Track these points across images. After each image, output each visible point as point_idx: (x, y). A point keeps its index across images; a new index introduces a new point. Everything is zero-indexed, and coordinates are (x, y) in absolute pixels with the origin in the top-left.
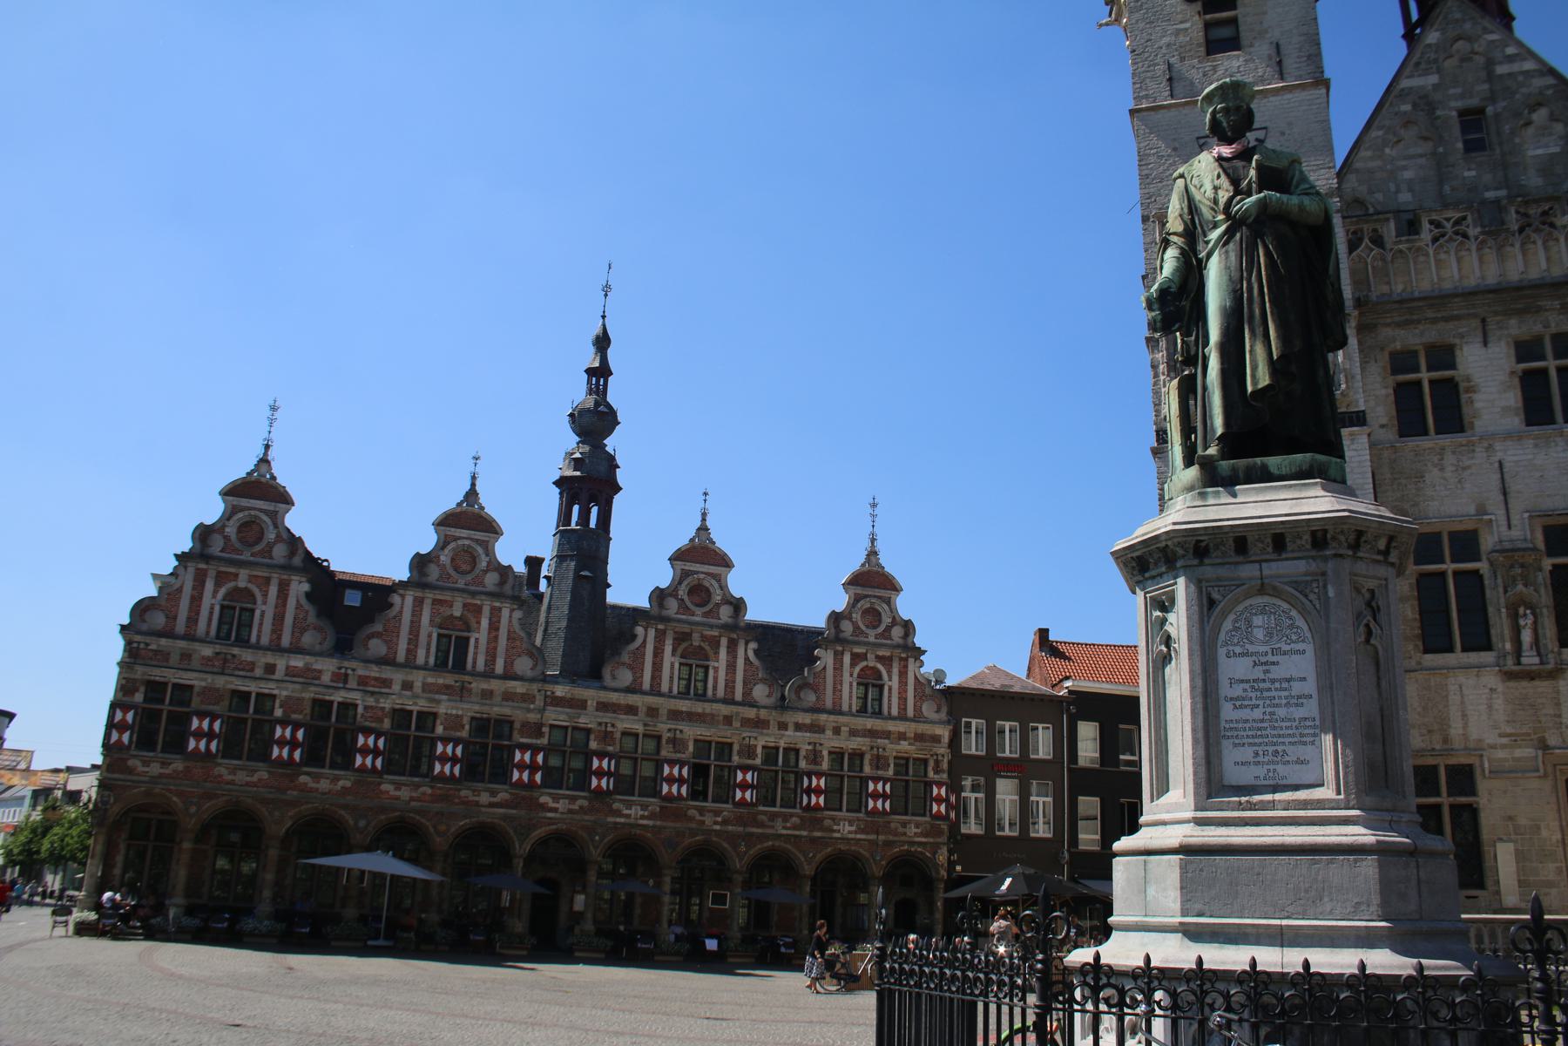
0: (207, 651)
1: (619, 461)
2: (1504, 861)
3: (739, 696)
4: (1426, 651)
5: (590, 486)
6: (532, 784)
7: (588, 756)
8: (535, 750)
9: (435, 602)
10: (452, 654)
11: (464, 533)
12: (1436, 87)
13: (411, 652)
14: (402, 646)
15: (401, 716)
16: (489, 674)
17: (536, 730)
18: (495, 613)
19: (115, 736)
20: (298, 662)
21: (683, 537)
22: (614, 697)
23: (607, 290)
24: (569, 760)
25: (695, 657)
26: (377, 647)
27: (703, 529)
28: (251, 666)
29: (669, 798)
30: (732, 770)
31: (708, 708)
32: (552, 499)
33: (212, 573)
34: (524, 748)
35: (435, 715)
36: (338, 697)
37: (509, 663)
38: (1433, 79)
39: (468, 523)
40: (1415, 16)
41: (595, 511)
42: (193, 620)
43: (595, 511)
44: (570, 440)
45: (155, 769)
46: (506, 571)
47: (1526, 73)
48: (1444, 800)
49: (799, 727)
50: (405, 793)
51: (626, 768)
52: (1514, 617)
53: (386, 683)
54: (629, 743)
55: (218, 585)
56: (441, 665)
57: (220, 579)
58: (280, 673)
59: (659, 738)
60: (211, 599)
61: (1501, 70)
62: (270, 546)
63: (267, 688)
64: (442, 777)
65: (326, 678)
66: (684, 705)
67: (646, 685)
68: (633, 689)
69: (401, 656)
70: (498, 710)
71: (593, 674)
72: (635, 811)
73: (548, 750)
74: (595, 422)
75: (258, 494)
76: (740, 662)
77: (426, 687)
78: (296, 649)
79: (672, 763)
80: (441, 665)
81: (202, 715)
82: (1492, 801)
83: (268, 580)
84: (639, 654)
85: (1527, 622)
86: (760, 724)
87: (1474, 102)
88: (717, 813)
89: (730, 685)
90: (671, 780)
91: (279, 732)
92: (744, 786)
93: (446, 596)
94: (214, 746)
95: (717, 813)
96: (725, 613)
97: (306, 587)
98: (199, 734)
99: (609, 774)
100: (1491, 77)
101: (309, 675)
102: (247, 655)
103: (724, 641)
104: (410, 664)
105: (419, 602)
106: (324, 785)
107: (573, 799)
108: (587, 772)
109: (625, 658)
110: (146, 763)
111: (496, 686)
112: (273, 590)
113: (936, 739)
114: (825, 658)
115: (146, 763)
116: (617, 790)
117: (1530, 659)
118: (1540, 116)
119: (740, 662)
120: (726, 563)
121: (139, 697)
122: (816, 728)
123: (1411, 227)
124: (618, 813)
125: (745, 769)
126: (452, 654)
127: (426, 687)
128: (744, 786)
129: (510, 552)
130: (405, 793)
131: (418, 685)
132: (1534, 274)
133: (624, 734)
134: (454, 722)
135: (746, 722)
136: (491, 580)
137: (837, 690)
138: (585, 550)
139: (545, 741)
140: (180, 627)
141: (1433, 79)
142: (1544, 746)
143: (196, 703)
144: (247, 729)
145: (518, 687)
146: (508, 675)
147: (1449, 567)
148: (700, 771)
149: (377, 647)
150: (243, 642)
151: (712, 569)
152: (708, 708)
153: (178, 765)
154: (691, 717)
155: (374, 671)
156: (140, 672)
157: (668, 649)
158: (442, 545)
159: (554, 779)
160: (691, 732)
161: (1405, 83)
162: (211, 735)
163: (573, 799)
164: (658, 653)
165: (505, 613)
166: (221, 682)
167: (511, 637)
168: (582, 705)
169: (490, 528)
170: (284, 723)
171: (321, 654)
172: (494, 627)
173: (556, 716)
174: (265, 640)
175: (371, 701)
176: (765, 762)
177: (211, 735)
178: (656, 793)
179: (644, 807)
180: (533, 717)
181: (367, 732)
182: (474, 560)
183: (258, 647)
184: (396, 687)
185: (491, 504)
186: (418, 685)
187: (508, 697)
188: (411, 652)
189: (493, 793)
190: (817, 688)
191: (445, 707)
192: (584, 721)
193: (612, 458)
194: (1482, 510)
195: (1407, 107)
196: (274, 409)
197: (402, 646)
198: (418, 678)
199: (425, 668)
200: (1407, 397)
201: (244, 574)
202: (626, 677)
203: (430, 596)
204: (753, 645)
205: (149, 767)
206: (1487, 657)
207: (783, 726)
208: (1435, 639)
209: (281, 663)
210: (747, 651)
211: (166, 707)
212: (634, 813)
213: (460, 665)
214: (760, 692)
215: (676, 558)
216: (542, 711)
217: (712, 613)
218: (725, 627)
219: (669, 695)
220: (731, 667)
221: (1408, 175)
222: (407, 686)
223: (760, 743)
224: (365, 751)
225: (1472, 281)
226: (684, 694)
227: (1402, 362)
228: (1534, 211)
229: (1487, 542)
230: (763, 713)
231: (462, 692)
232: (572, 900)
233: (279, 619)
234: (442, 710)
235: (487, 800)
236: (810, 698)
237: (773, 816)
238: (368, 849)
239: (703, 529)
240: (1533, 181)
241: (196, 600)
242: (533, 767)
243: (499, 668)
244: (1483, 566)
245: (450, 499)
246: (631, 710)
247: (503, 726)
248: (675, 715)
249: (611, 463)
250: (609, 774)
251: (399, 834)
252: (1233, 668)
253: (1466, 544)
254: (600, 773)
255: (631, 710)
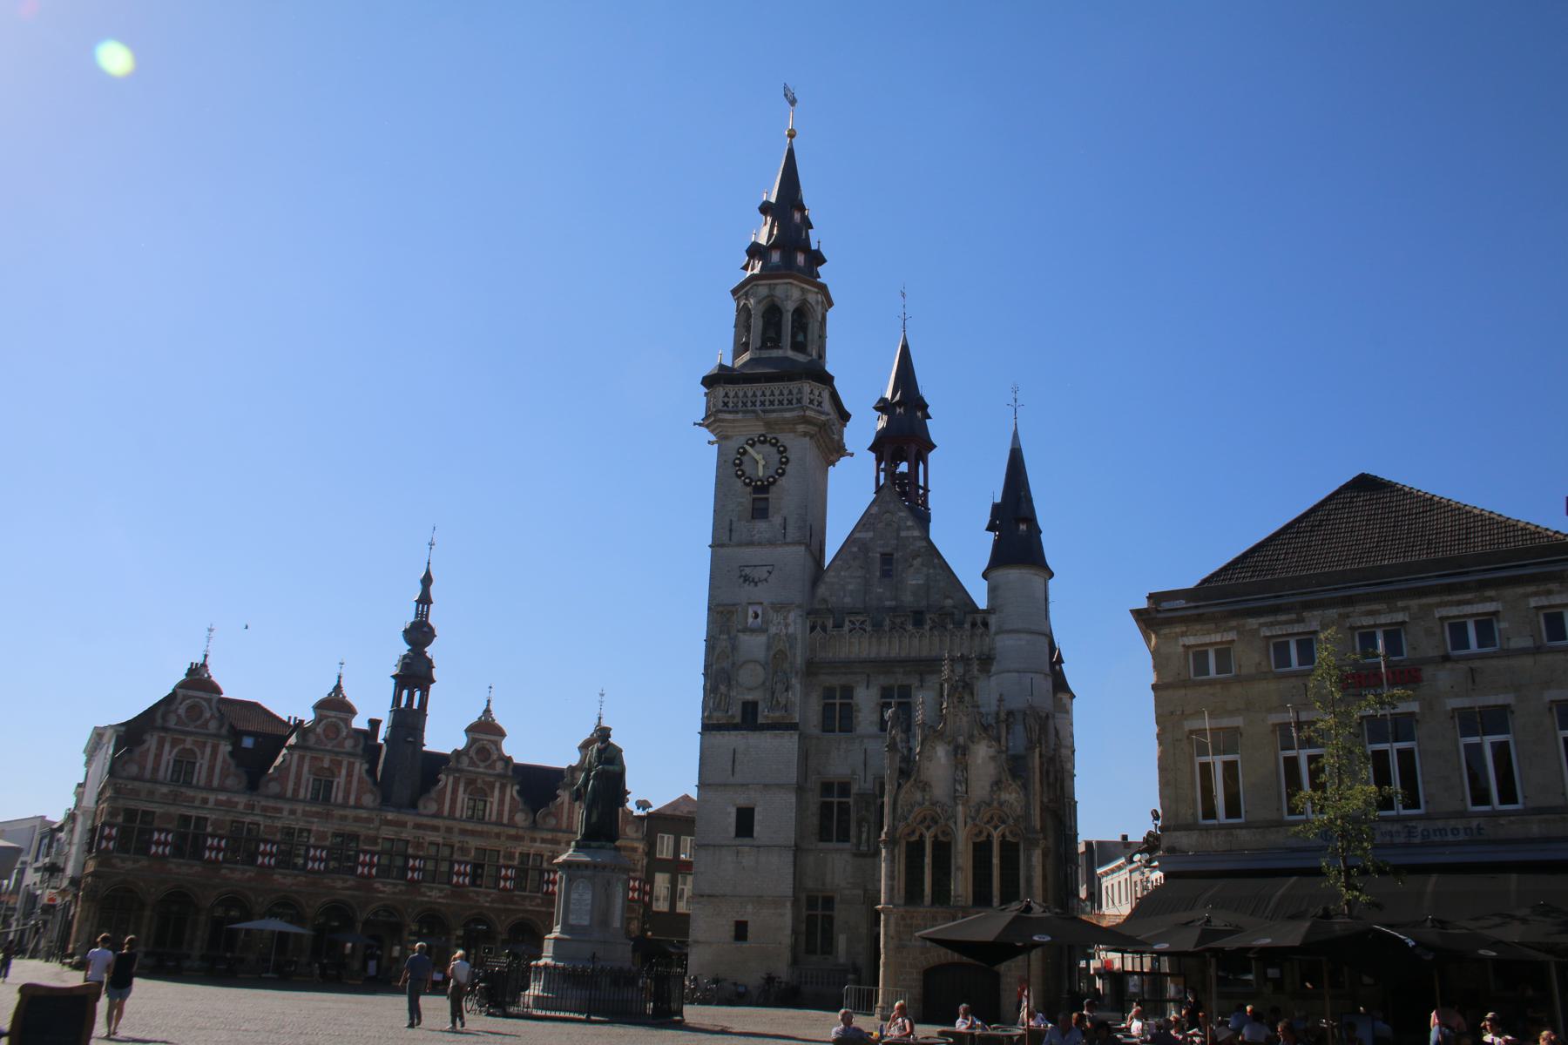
0: (165, 790)
1: (435, 663)
2: (841, 941)
3: (505, 820)
4: (821, 840)
5: (415, 674)
6: (370, 876)
7: (407, 857)
8: (373, 854)
9: (314, 759)
10: (323, 790)
11: (333, 713)
12: (871, 539)
13: (296, 791)
14: (290, 786)
15: (289, 832)
16: (345, 805)
17: (373, 840)
18: (351, 765)
19: (104, 844)
20: (223, 797)
21: (474, 716)
22: (425, 820)
23: (431, 544)
24: (395, 860)
25: (479, 793)
26: (274, 788)
27: (487, 711)
28: (193, 799)
29: (457, 885)
30: (499, 869)
31: (485, 828)
32: (391, 684)
33: (169, 739)
34: (365, 852)
35: (309, 831)
36: (247, 819)
37: (358, 799)
38: (870, 534)
39: (335, 706)
40: (882, 482)
41: (417, 694)
42: (156, 769)
43: (417, 694)
44: (404, 648)
45: (129, 865)
46: (358, 731)
47: (915, 538)
48: (819, 912)
49: (543, 841)
50: (289, 881)
51: (430, 865)
52: (859, 826)
53: (280, 810)
54: (433, 850)
55: (173, 746)
56: (315, 799)
57: (174, 743)
58: (211, 805)
59: (452, 847)
60: (168, 756)
61: (903, 534)
62: (207, 722)
63: (203, 813)
64: (312, 871)
65: (241, 807)
66: (470, 826)
67: (446, 813)
68: (435, 816)
69: (289, 793)
70: (351, 827)
71: (413, 805)
72: (434, 893)
73: (380, 854)
74: (420, 634)
75: (197, 680)
76: (508, 798)
77: (305, 813)
78: (222, 789)
79: (460, 863)
80: (315, 799)
81: (160, 831)
82: (840, 914)
83: (204, 744)
84: (443, 791)
85: (865, 829)
86: (518, 838)
87: (888, 550)
88: (488, 895)
89: (500, 813)
90: (459, 874)
91: (209, 841)
92: (506, 878)
93: (319, 755)
94: (167, 850)
95: (488, 895)
96: (499, 766)
97: (229, 748)
98: (158, 843)
99: (419, 869)
100: (898, 537)
101: (231, 805)
102: (190, 793)
103: (497, 785)
104: (294, 799)
105: (302, 758)
106: (237, 875)
107: (395, 885)
108: (405, 868)
109: (433, 794)
110: (123, 861)
111: (349, 813)
112: (208, 751)
113: (635, 850)
114: (564, 796)
115: (123, 861)
116: (424, 880)
117: (864, 848)
118: (917, 562)
119: (508, 798)
120: (502, 734)
121: (120, 819)
122: (556, 842)
123: (838, 626)
124: (424, 895)
125: (507, 867)
126: (323, 790)
127: (305, 813)
128: (506, 878)
129: (360, 723)
130: (289, 881)
131: (299, 811)
132: (893, 654)
133: (431, 843)
134: (322, 836)
135: (510, 837)
136: (349, 744)
137: (570, 817)
138: (409, 722)
139: (378, 848)
140: (148, 774)
141: (870, 534)
142: (865, 891)
143: (156, 824)
144: (190, 840)
145: (364, 814)
146: (358, 806)
147: (836, 800)
148: (477, 867)
149: (274, 788)
150: (188, 784)
151: (493, 738)
152: (485, 828)
153: (144, 862)
154: (473, 833)
155: (271, 803)
156: (121, 803)
157: (461, 789)
158: (318, 721)
159: (384, 872)
160: (473, 843)
161: (857, 535)
162: (166, 844)
163: (395, 885)
164: (455, 791)
165: (357, 766)
166: (172, 809)
167: (360, 780)
168: (404, 825)
169: (350, 711)
170: (213, 836)
171: (236, 792)
172: (349, 774)
173: (387, 832)
174: (202, 783)
175: (269, 822)
176: (522, 862)
177: (166, 844)
178: (449, 882)
179: (441, 890)
180: (372, 833)
181: (266, 842)
182: (338, 731)
183: (197, 787)
184: (285, 813)
185: (350, 694)
186: (299, 811)
187: (357, 819)
188: (296, 791)
189: (345, 881)
190: (557, 816)
191: (316, 826)
192: (404, 836)
193: (430, 662)
194: (854, 773)
195: (855, 549)
196: (210, 630)
197: (290, 786)
198: (300, 808)
199: (303, 801)
200: (828, 709)
201: (189, 739)
202: (433, 807)
203: (309, 755)
204: (516, 787)
205: (127, 865)
206: (847, 845)
207: (533, 840)
208: (824, 834)
209: (212, 798)
210: (512, 791)
211: (137, 824)
212: (434, 895)
213: (327, 799)
214: (520, 818)
215: (468, 731)
216: (378, 829)
217: (492, 766)
218: (499, 776)
219: (460, 820)
220: (502, 802)
221: (851, 587)
222: (293, 812)
223: (518, 850)
224: (264, 854)
225: (864, 655)
226: (470, 819)
227: (829, 693)
228: (898, 621)
229: (855, 789)
230: (521, 832)
231: (327, 816)
232: (391, 951)
233: (211, 768)
234: (314, 828)
235: (342, 886)
236: (552, 822)
237: (524, 898)
238: (262, 917)
239: (487, 711)
240: (908, 598)
241: (158, 756)
242: (371, 865)
243: (352, 801)
244: (851, 801)
245: (324, 692)
246: (436, 829)
247: (354, 837)
248: (464, 832)
249: (429, 664)
250: (419, 869)
251: (285, 906)
252: (574, 896)
253: (845, 788)
254: (414, 869)
255: (436, 829)
